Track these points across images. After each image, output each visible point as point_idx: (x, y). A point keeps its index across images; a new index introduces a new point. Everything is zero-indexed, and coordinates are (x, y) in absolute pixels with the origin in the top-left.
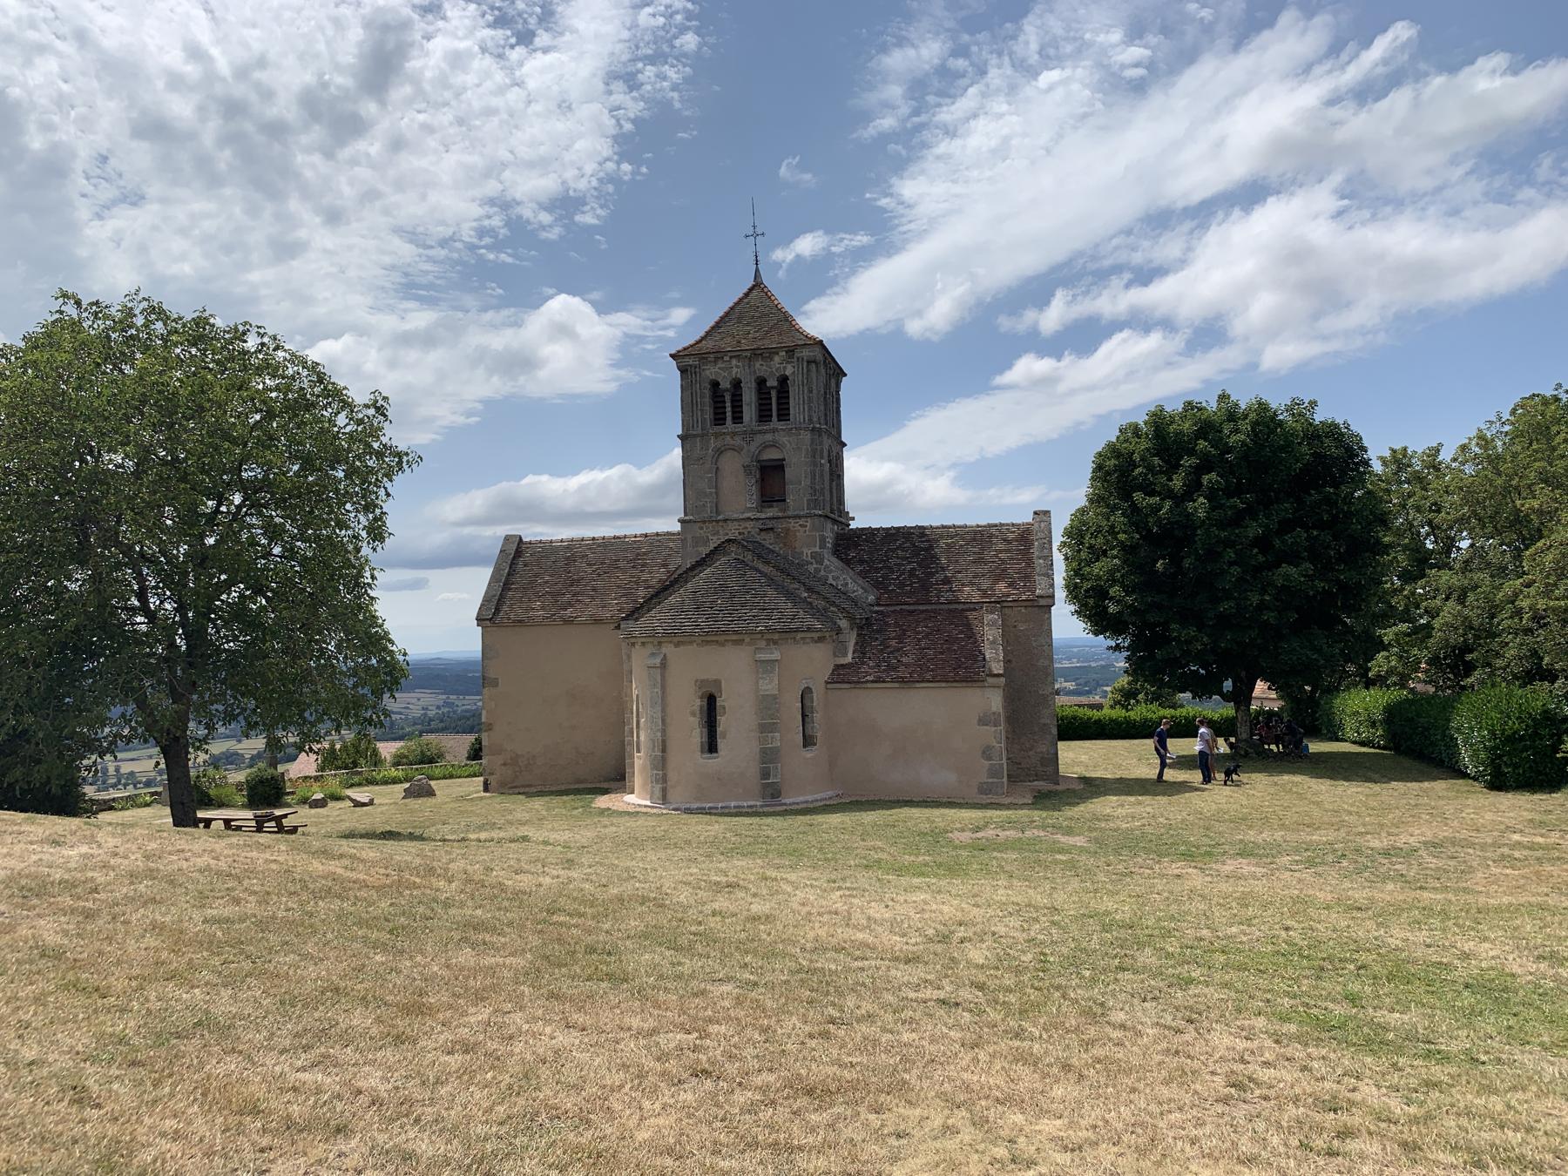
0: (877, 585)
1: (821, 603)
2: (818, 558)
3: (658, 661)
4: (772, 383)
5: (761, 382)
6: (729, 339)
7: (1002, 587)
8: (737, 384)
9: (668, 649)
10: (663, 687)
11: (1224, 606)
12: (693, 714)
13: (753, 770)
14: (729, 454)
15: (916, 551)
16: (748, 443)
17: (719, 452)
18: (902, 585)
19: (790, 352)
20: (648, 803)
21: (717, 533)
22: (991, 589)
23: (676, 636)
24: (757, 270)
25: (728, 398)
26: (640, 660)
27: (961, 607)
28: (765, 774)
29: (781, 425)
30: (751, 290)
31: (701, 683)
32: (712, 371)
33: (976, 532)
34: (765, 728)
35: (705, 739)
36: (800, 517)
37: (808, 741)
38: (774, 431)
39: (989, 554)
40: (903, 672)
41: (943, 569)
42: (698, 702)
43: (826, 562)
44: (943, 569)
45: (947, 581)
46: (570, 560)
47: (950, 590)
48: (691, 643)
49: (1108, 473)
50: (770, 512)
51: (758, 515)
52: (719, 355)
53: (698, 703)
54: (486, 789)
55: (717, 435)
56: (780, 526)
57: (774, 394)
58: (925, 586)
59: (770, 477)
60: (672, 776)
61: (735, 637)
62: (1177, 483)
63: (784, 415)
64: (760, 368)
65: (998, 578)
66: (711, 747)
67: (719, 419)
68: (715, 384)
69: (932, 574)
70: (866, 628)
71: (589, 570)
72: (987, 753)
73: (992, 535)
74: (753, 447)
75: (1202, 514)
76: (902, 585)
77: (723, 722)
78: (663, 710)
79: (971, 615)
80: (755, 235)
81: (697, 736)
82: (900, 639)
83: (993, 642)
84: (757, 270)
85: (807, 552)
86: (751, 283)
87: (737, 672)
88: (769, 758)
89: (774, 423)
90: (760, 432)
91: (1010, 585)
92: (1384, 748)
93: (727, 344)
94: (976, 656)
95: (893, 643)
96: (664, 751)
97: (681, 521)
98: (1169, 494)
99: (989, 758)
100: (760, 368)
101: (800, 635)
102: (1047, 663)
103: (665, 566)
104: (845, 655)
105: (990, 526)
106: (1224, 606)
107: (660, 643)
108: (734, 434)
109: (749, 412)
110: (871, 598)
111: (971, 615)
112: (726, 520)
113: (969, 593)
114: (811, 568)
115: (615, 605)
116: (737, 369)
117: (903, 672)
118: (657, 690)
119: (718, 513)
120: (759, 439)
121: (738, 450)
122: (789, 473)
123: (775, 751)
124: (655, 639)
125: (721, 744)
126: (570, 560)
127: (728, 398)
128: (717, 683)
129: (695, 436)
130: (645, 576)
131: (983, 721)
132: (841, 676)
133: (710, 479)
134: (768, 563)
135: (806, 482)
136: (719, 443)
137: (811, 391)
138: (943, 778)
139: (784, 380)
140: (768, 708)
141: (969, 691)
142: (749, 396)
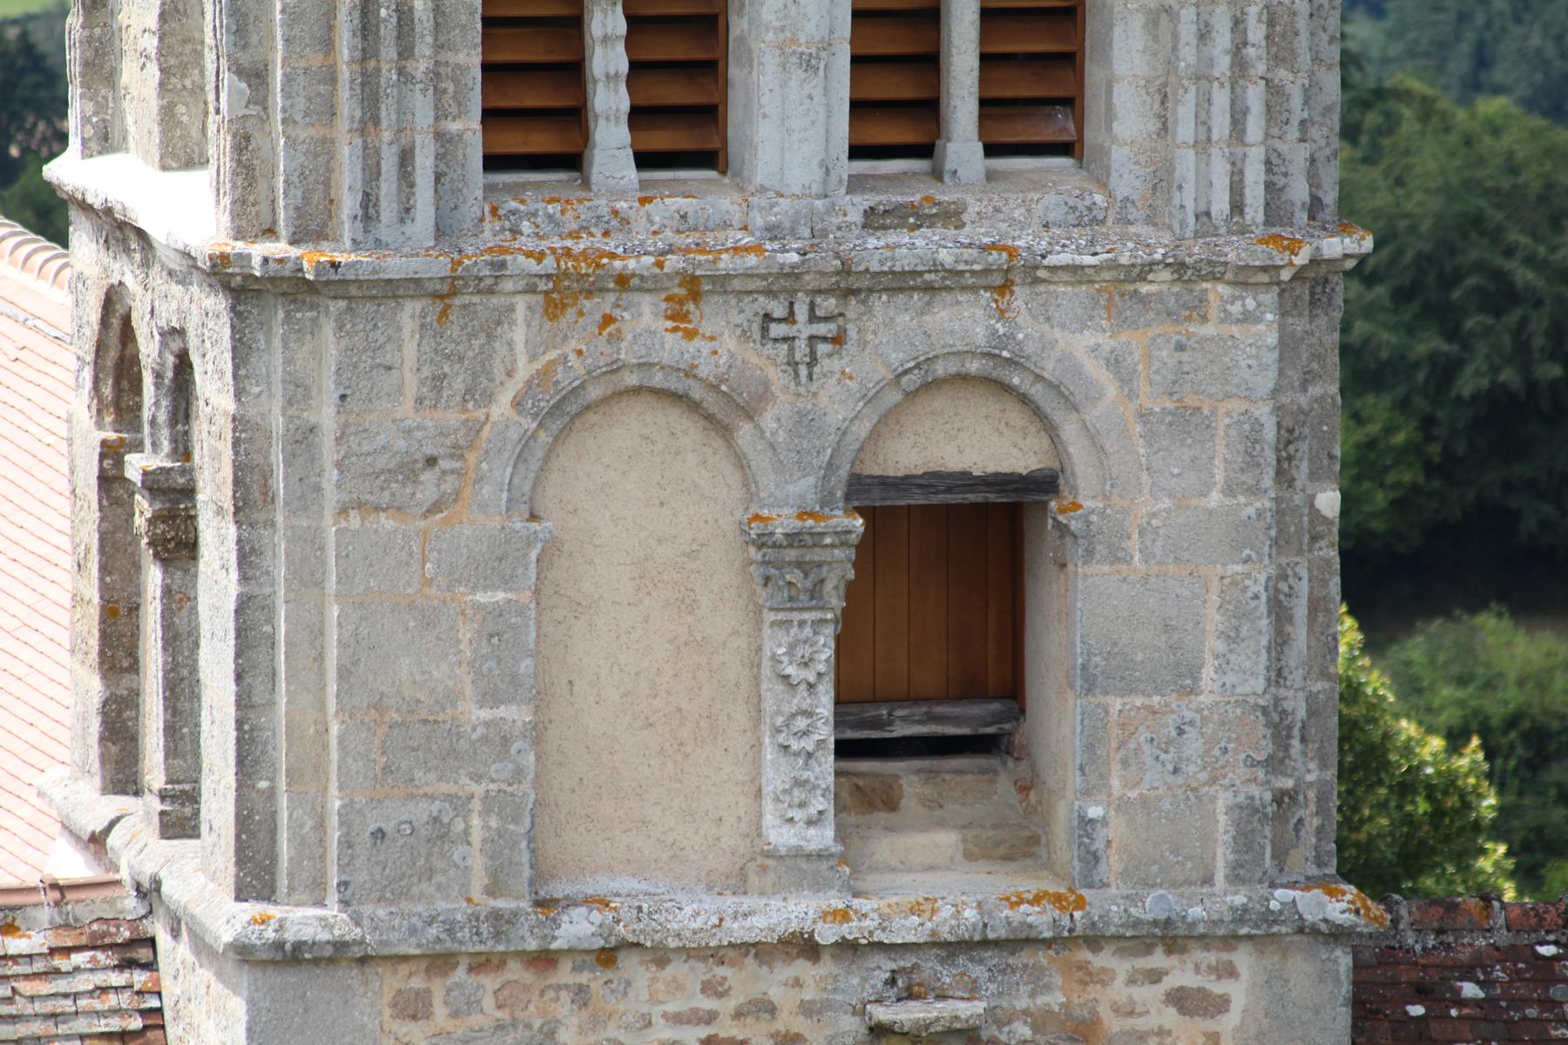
17: (564, 412)
36: (1170, 936)
38: (1005, 277)
55: (560, 292)
67: (533, 120)
74: (840, 395)
90: (900, 283)
112: (607, 956)
120: (890, 335)
121: (716, 410)
129: (391, 290)
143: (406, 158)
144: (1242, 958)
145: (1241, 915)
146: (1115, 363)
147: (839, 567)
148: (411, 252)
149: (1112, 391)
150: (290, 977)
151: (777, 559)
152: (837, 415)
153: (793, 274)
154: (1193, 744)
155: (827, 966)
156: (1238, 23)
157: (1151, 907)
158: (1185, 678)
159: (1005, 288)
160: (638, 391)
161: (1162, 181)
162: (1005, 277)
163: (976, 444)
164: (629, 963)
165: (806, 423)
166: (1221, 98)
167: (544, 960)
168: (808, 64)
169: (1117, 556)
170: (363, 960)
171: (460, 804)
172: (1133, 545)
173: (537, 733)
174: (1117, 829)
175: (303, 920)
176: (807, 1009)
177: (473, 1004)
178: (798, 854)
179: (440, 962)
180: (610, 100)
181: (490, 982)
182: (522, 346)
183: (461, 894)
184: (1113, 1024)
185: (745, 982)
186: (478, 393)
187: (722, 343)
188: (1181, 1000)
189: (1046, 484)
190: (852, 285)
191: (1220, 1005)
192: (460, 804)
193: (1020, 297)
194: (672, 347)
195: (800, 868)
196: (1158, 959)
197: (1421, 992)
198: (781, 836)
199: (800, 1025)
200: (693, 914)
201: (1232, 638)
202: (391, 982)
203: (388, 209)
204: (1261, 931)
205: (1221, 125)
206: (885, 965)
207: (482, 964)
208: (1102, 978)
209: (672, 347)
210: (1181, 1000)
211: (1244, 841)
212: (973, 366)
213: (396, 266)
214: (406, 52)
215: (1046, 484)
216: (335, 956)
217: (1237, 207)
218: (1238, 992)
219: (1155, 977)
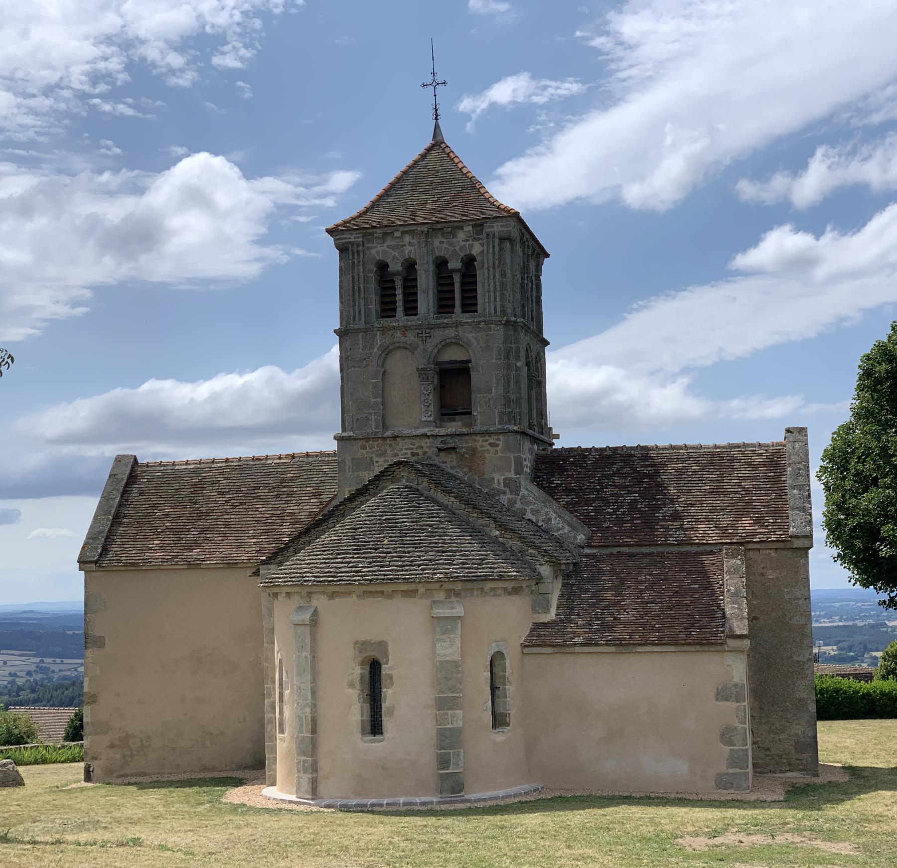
0: (588, 521)
1: (516, 544)
2: (513, 486)
3: (306, 616)
4: (455, 264)
5: (441, 264)
6: (401, 211)
7: (746, 524)
8: (410, 266)
9: (320, 602)
10: (314, 651)
12: (351, 685)
13: (428, 757)
16: (424, 341)
17: (387, 351)
18: (620, 521)
19: (479, 226)
20: (293, 798)
21: (384, 454)
22: (733, 526)
23: (332, 585)
24: (437, 127)
25: (399, 284)
26: (284, 616)
27: (694, 549)
28: (444, 762)
29: (466, 318)
30: (429, 150)
31: (362, 646)
32: (378, 250)
33: (713, 455)
34: (445, 703)
35: (367, 717)
36: (489, 433)
37: (499, 720)
38: (457, 325)
39: (730, 483)
40: (621, 632)
41: (672, 501)
42: (358, 670)
43: (523, 492)
44: (672, 501)
45: (676, 516)
46: (198, 487)
47: (681, 528)
48: (349, 594)
49: (878, 381)
50: (453, 427)
51: (437, 431)
52: (388, 230)
53: (357, 671)
54: (88, 777)
55: (384, 330)
56: (464, 445)
57: (457, 278)
58: (649, 522)
59: (451, 385)
60: (325, 765)
61: (405, 587)
64: (440, 246)
65: (740, 514)
66: (375, 727)
67: (387, 309)
68: (383, 267)
69: (658, 508)
70: (573, 575)
71: (221, 500)
72: (727, 736)
73: (733, 459)
74: (431, 345)
76: (620, 521)
77: (389, 695)
78: (314, 681)
79: (707, 560)
80: (435, 84)
81: (356, 713)
83: (736, 594)
84: (437, 127)
85: (499, 479)
86: (429, 141)
87: (409, 633)
88: (448, 742)
89: (458, 314)
90: (440, 326)
93: (399, 217)
94: (714, 612)
95: (609, 595)
96: (314, 731)
97: (338, 438)
99: (730, 743)
100: (440, 246)
101: (489, 585)
103: (316, 495)
104: (547, 610)
105: (732, 447)
107: (309, 594)
108: (405, 329)
109: (426, 302)
110: (581, 538)
111: (707, 560)
112: (395, 438)
113: (705, 532)
114: (504, 499)
115: (252, 545)
116: (411, 248)
117: (621, 632)
118: (306, 654)
119: (385, 427)
120: (439, 335)
121: (411, 349)
122: (475, 377)
124: (307, 589)
125: (387, 723)
126: (198, 487)
127: (399, 284)
128: (382, 645)
129: (357, 331)
130: (292, 508)
131: (723, 695)
132: (542, 637)
134: (449, 492)
135: (497, 390)
137: (503, 275)
138: (672, 768)
139: (469, 262)
140: (448, 676)
142: (426, 281)
143: (360, 311)
144: (501, 437)
145: (499, 429)
146: (476, 339)
148: (361, 324)
149: (476, 343)
150: (344, 442)
151: (421, 371)
152: (430, 349)
153: (421, 325)
154: (491, 402)
155: (431, 439)
156: (495, 283)
157: (485, 428)
158: (489, 391)
159: (457, 326)
160: (403, 348)
162: (457, 325)
163: (454, 355)
164: (398, 439)
165: (424, 350)
166: (492, 294)
167: (384, 439)
168: (424, 292)
169: (478, 371)
170: (355, 439)
171: (370, 414)
172: (480, 369)
173: (383, 403)
174: (479, 417)
175: (345, 434)
176: (428, 447)
177: (373, 447)
178: (426, 421)
179: (367, 439)
180: (400, 304)
181: (376, 443)
182: (379, 340)
184: (480, 449)
186: (372, 348)
187: (411, 337)
188: (491, 444)
189: (469, 361)
190: (431, 327)
191: (498, 445)
192: (370, 414)
193: (460, 329)
194: (403, 339)
195: (426, 424)
196: (487, 438)
197: (562, 460)
198: (424, 419)
199: (427, 450)
200: (406, 432)
201: (497, 384)
202: (360, 443)
203: (357, 319)
204: (503, 432)
205: (492, 299)
206: (440, 439)
207: (375, 439)
208: (478, 441)
209: (403, 339)
210: (491, 444)
211: (501, 418)
212: (453, 340)
213: (356, 327)
214: (359, 294)
215: (469, 361)
216: (349, 439)
217: (496, 312)
218: (501, 443)
219: (487, 441)
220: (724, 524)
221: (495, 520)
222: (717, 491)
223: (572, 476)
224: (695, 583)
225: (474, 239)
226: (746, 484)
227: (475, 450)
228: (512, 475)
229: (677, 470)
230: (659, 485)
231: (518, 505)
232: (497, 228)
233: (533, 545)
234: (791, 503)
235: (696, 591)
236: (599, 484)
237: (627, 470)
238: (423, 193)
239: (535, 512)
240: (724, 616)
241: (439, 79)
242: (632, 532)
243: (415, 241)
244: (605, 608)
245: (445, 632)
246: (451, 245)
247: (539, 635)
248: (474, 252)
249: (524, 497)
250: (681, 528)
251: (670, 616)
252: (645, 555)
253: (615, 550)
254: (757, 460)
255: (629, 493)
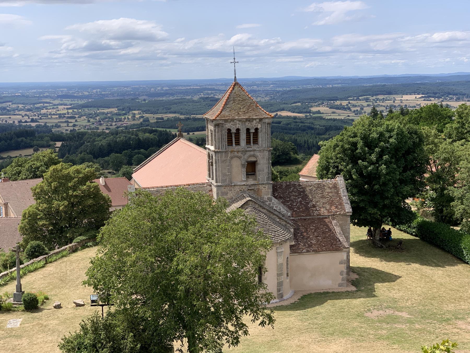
2: (270, 200)
8: (238, 130)
11: (387, 202)
14: (235, 159)
15: (300, 193)
17: (232, 158)
18: (299, 208)
19: (261, 120)
21: (231, 190)
22: (330, 209)
24: (235, 77)
27: (321, 217)
28: (279, 290)
32: (228, 126)
34: (279, 275)
36: (263, 184)
38: (254, 151)
40: (315, 248)
41: (311, 201)
43: (273, 201)
45: (314, 206)
47: (316, 210)
49: (346, 150)
57: (252, 135)
58: (307, 209)
62: (373, 157)
63: (256, 141)
67: (230, 143)
68: (229, 130)
69: (308, 203)
72: (341, 273)
74: (246, 157)
75: (384, 171)
79: (327, 220)
80: (235, 62)
82: (306, 231)
84: (235, 77)
85: (266, 197)
88: (280, 284)
90: (249, 151)
91: (336, 207)
92: (416, 236)
94: (336, 240)
95: (305, 234)
98: (371, 163)
99: (342, 275)
100: (248, 125)
102: (348, 235)
106: (387, 202)
109: (243, 142)
110: (289, 214)
111: (327, 220)
112: (234, 186)
113: (323, 212)
114: (267, 203)
117: (315, 248)
120: (248, 154)
121: (239, 158)
123: (282, 282)
129: (223, 152)
131: (341, 263)
133: (228, 169)
134: (264, 208)
136: (232, 155)
137: (268, 135)
139: (257, 129)
140: (280, 267)
141: (337, 253)
142: (243, 136)
147: (246, 165)
151: (243, 165)
161: (262, 146)
162: (254, 151)
163: (253, 159)
175: (219, 184)
179: (226, 186)
180: (234, 142)
183: (227, 182)
185: (241, 187)
187: (240, 154)
189: (256, 161)
190: (246, 151)
195: (244, 181)
200: (239, 183)
204: (268, 184)
215: (256, 161)
220: (328, 208)
221: (278, 217)
222: (323, 197)
223: (280, 192)
224: (326, 229)
225: (259, 123)
226: (330, 194)
227: (259, 189)
228: (270, 196)
229: (310, 190)
230: (306, 195)
231: (271, 205)
232: (267, 121)
233: (289, 223)
234: (344, 201)
235: (328, 232)
236: (289, 195)
237: (295, 190)
238: (238, 104)
239: (276, 207)
240: (340, 241)
241: (236, 60)
242: (303, 212)
243: (240, 123)
244: (306, 239)
245: (280, 256)
246: (252, 125)
247: (293, 250)
248: (258, 127)
249: (273, 203)
250: (316, 210)
251: (325, 241)
252: (309, 219)
253: (299, 218)
254: (331, 186)
255: (299, 198)
